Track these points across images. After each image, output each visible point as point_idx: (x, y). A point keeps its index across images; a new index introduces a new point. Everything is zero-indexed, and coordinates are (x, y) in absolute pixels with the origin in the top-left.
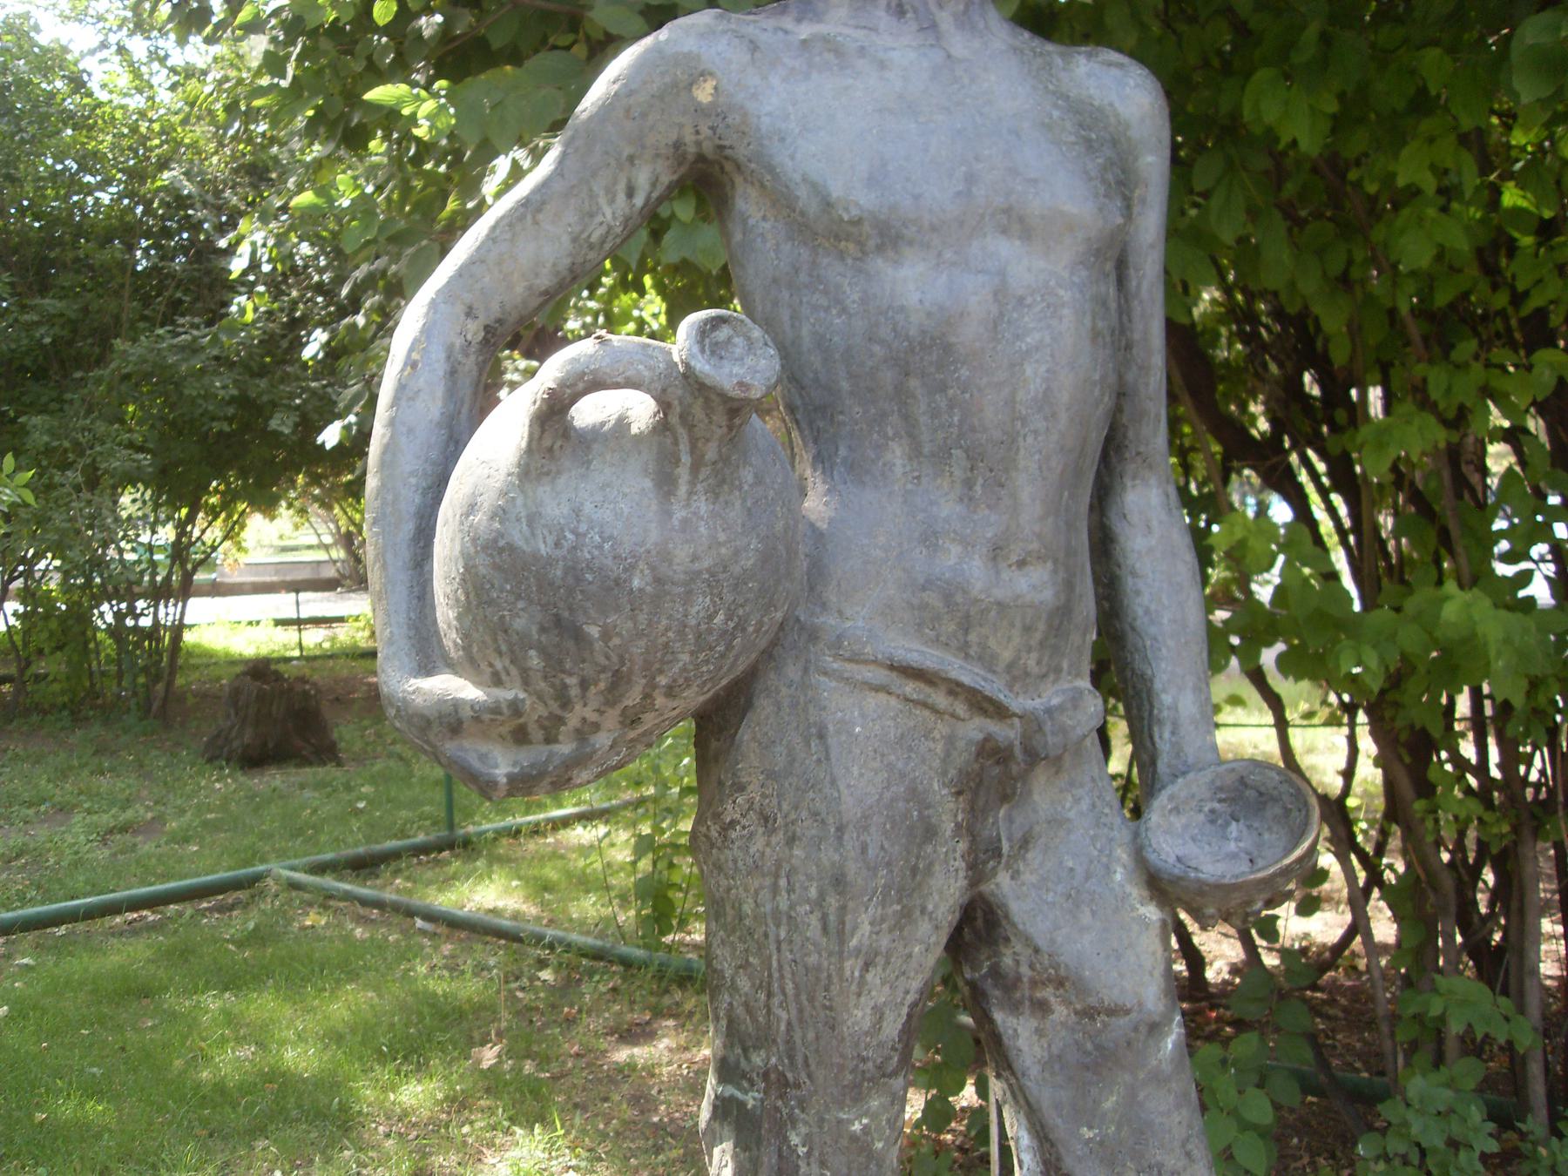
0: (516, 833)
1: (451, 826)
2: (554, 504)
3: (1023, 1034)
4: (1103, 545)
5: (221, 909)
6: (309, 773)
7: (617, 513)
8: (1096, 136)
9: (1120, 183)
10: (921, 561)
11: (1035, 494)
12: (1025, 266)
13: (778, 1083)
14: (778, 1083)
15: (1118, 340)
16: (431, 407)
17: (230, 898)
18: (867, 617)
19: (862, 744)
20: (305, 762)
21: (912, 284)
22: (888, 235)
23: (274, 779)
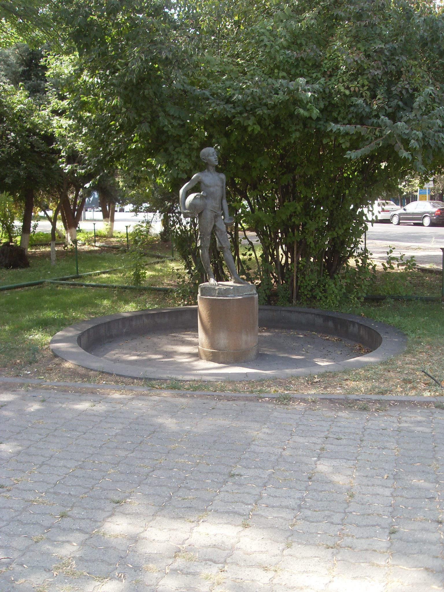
0: (90, 275)
1: (78, 273)
2: (195, 201)
3: (217, 233)
4: (222, 204)
5: (38, 288)
6: (23, 270)
7: (198, 202)
8: (222, 180)
9: (223, 183)
10: (212, 204)
11: (218, 201)
12: (217, 188)
13: (204, 235)
14: (204, 235)
15: (222, 191)
16: (184, 196)
17: (37, 286)
18: (209, 207)
19: (209, 215)
20: (23, 268)
21: (212, 189)
22: (210, 187)
23: (20, 271)
